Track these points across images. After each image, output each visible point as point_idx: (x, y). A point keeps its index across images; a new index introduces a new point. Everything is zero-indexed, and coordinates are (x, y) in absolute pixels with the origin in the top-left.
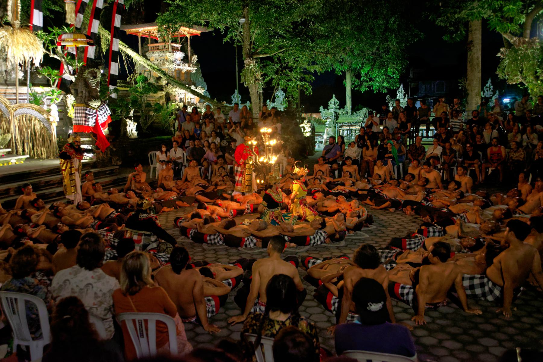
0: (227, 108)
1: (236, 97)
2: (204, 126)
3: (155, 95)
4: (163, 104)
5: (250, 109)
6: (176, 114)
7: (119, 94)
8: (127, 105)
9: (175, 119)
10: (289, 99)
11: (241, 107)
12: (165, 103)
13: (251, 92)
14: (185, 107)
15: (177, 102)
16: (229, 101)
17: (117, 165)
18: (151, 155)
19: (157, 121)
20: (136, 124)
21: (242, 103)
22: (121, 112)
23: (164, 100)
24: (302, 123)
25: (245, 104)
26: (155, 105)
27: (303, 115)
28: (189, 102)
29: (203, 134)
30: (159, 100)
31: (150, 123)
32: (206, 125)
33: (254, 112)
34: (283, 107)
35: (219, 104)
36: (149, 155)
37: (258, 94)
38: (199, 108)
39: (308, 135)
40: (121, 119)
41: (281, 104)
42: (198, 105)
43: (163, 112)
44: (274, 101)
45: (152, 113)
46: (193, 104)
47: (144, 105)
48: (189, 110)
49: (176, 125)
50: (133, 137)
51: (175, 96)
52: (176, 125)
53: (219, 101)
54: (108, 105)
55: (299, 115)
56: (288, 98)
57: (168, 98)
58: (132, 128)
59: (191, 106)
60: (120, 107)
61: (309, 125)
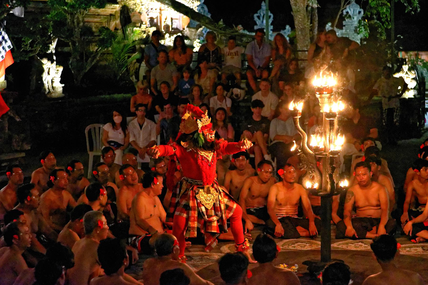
0: (244, 39)
1: (264, 19)
2: (196, 77)
3: (100, 11)
4: (116, 29)
5: (293, 40)
6: (142, 51)
7: (29, 10)
8: (45, 29)
9: (139, 61)
10: (372, 22)
11: (271, 36)
12: (120, 27)
13: (293, 7)
14: (158, 35)
15: (143, 27)
16: (249, 25)
17: (21, 151)
18: (90, 132)
19: (103, 63)
20: (61, 69)
21: (273, 30)
22: (32, 45)
23: (118, 21)
24: (399, 69)
25: (282, 32)
26: (100, 31)
27: (401, 55)
28: (167, 27)
29: (196, 92)
30: (109, 22)
31: (88, 68)
32: (200, 73)
33: (299, 47)
34: (359, 36)
35: (228, 31)
36: (86, 132)
37: (310, 12)
38: (187, 38)
39: (409, 94)
40: (32, 58)
41: (355, 31)
42: (187, 32)
43: (115, 45)
44: (340, 26)
45: (94, 48)
46: (176, 30)
47: (77, 31)
48: (168, 41)
49: (142, 73)
50: (54, 95)
51: (140, 13)
52: (142, 73)
53: (229, 24)
54: (7, 32)
55: (392, 53)
56: (370, 19)
57: (127, 17)
58: (52, 76)
59: (171, 34)
60: (31, 34)
61: (413, 74)
